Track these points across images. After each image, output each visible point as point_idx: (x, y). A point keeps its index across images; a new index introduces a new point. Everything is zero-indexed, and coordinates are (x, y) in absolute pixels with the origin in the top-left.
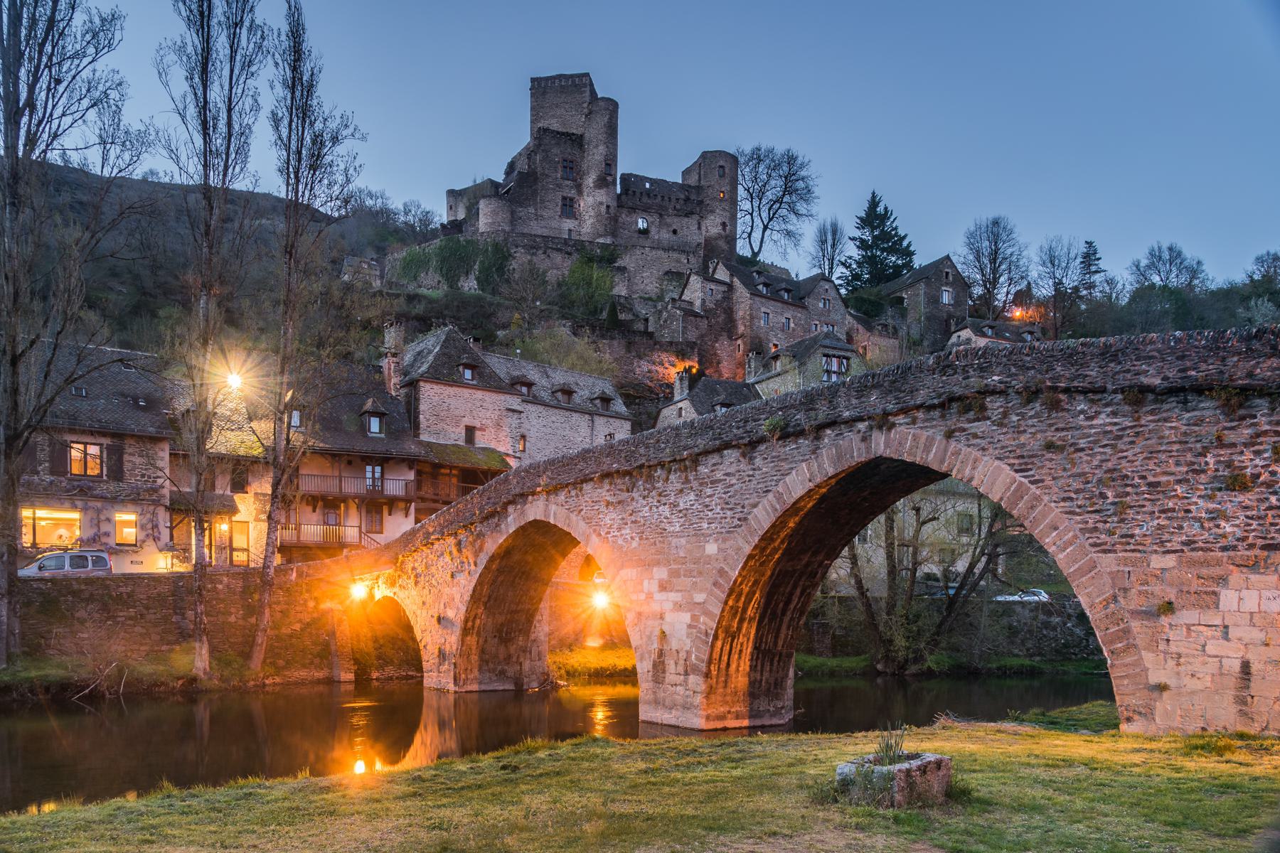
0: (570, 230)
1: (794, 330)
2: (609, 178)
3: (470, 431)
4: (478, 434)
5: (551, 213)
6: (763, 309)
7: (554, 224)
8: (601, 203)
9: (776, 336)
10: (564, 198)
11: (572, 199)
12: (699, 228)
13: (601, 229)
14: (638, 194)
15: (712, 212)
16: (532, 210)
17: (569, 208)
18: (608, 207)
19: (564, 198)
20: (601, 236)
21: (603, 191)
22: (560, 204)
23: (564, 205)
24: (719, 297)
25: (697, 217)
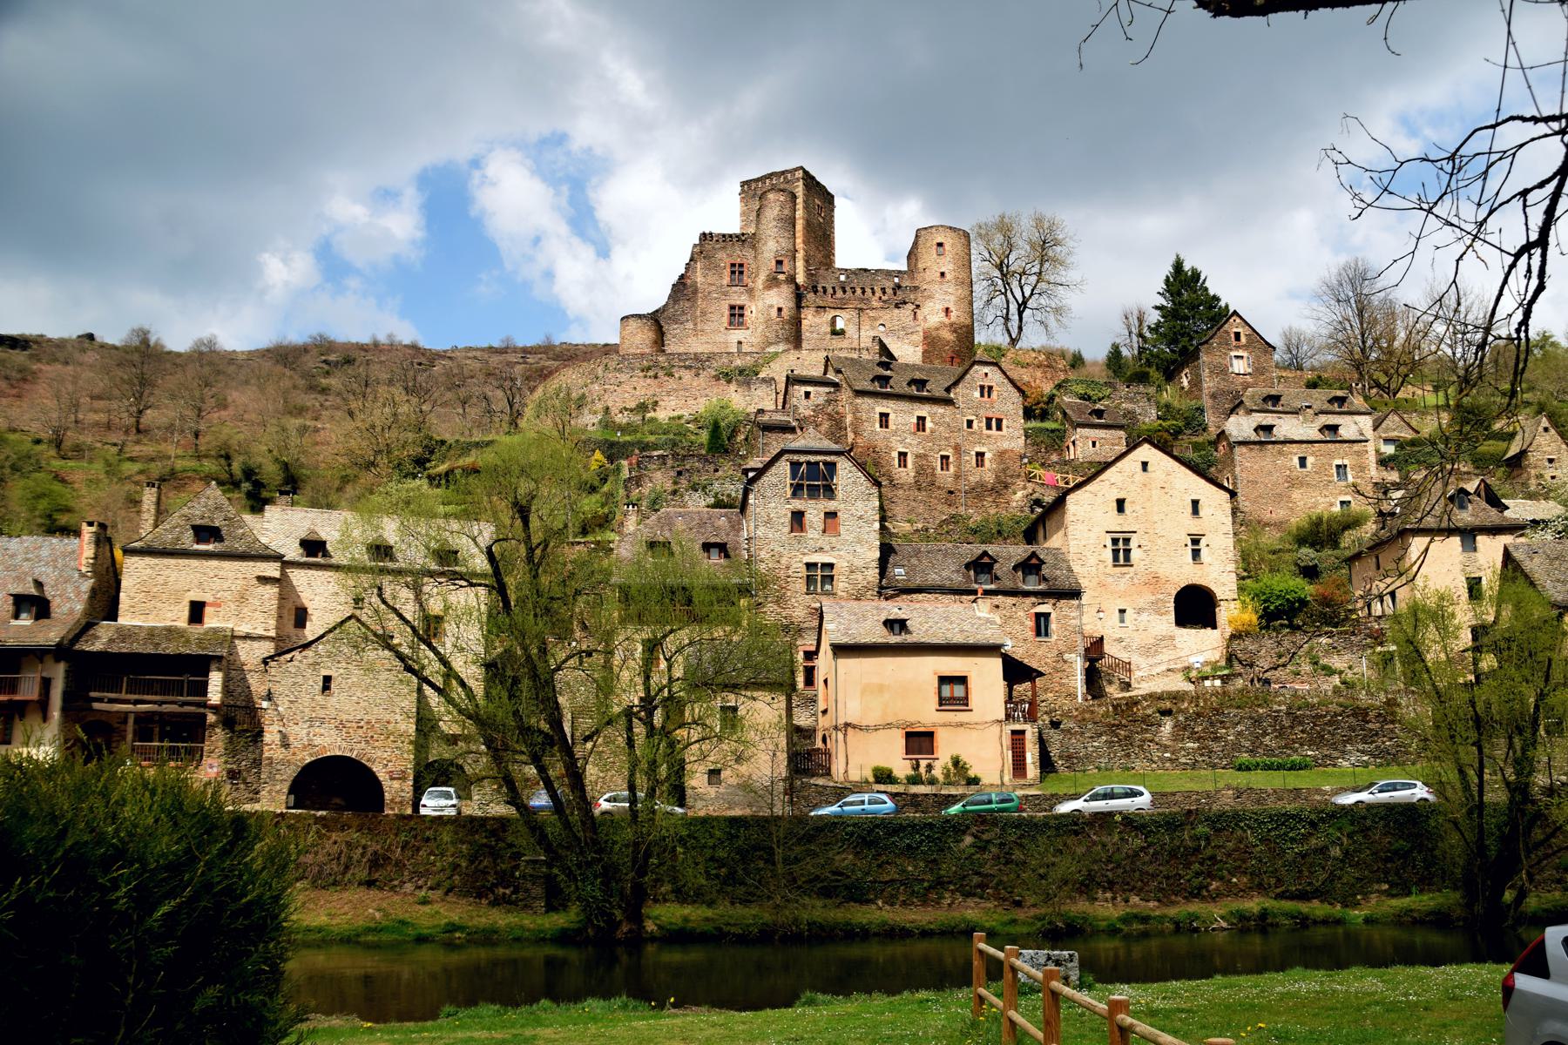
0: (740, 343)
1: (932, 432)
2: (782, 277)
3: (197, 611)
4: (208, 610)
5: (713, 326)
6: (879, 409)
7: (720, 338)
8: (771, 306)
9: (901, 442)
10: (732, 307)
11: (741, 308)
12: (915, 318)
13: (772, 336)
14: (830, 291)
15: (930, 297)
16: (690, 325)
17: (737, 314)
18: (780, 310)
19: (732, 307)
20: (771, 344)
21: (774, 292)
22: (727, 313)
23: (732, 315)
24: (821, 400)
25: (911, 307)
